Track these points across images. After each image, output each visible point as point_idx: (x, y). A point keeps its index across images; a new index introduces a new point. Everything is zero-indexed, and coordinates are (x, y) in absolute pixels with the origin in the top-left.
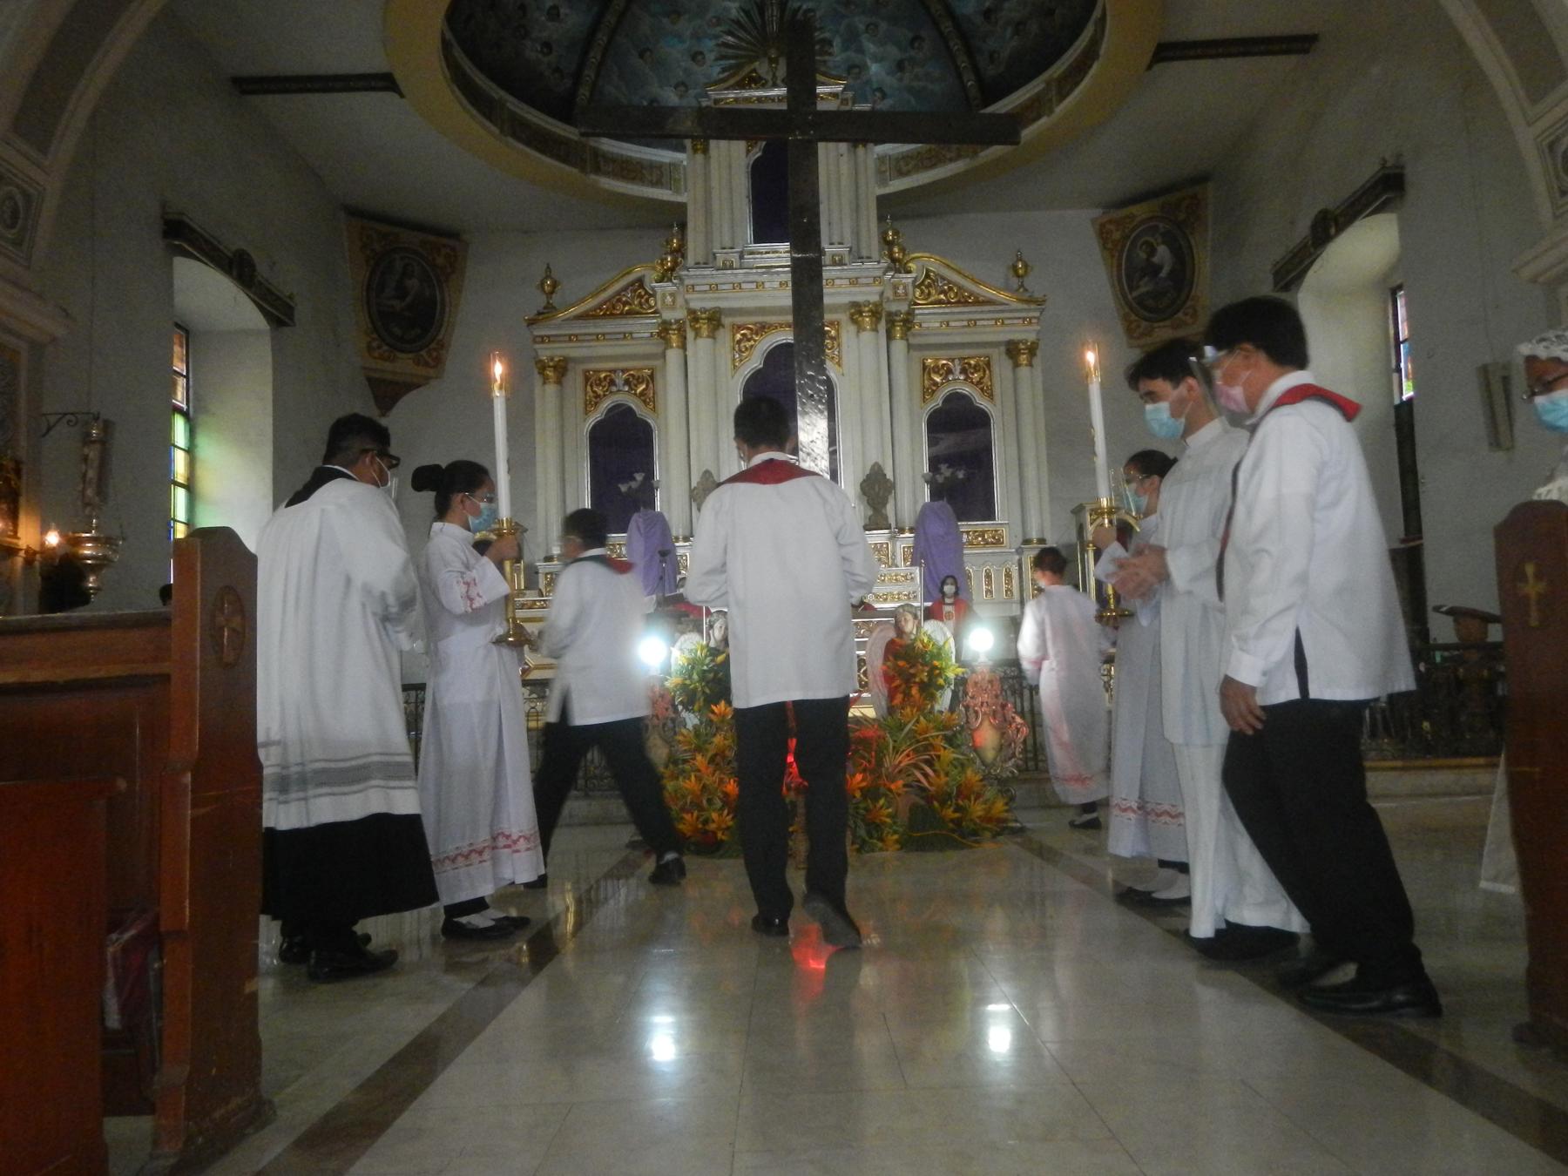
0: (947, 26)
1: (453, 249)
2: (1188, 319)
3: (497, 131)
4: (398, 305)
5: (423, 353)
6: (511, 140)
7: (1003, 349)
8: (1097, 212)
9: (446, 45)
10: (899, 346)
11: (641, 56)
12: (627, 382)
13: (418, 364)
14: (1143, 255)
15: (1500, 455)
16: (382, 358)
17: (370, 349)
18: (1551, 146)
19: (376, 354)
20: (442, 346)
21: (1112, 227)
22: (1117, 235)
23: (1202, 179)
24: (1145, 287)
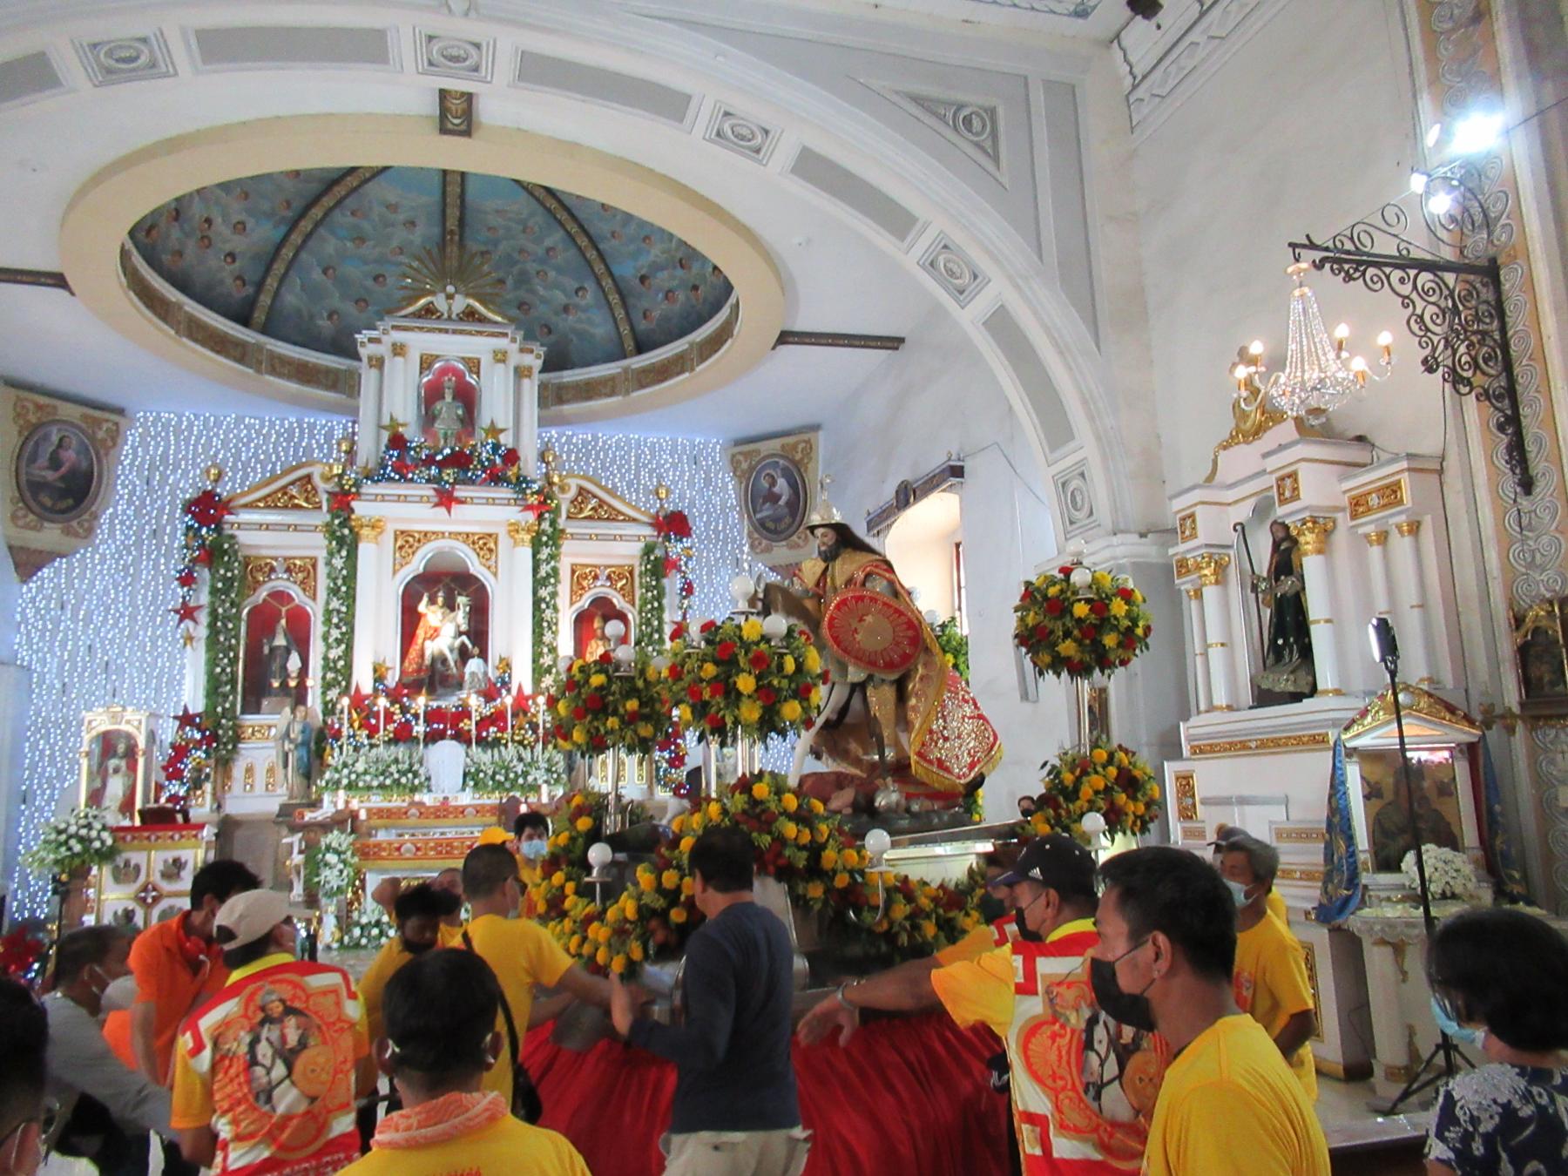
0: (607, 283)
1: (116, 424)
2: (801, 542)
3: (172, 332)
5: (74, 523)
6: (185, 340)
9: (124, 254)
11: (325, 272)
12: (288, 570)
15: (1027, 706)
16: (27, 527)
17: (14, 518)
18: (1064, 485)
19: (21, 523)
20: (96, 517)
21: (741, 458)
22: (745, 466)
23: (815, 428)
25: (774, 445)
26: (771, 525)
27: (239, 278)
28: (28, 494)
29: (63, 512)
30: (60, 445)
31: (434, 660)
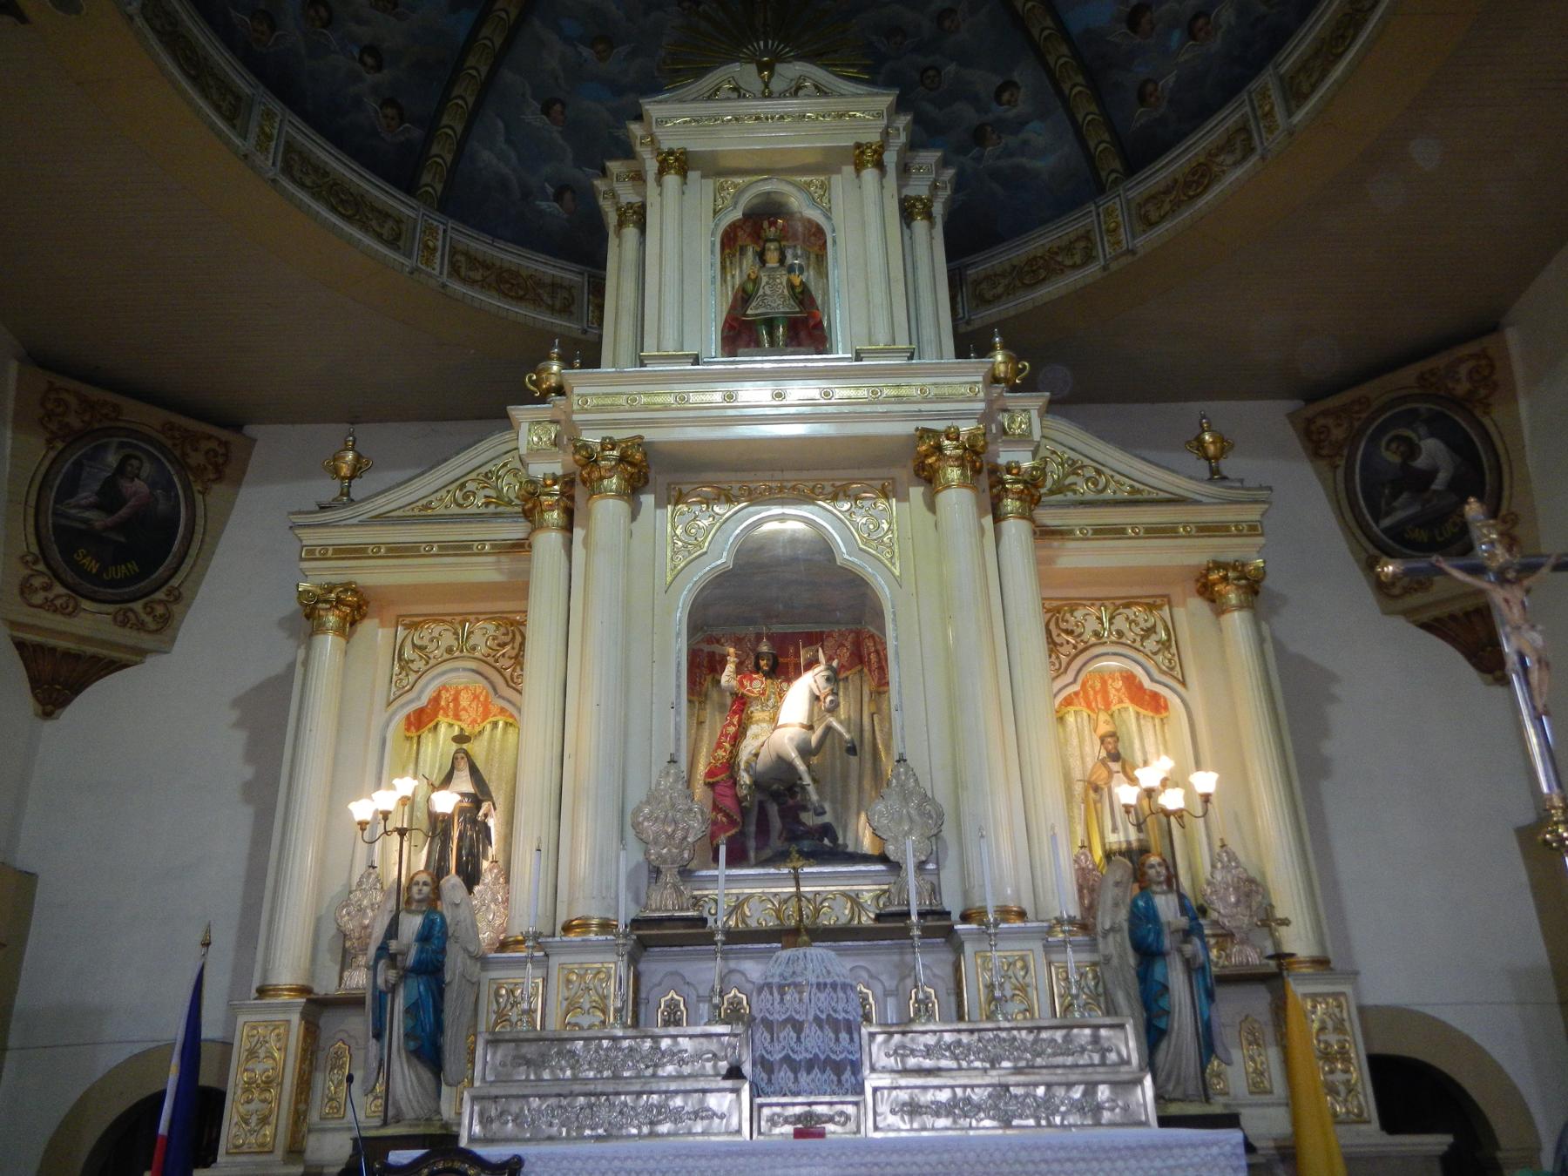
0: (1059, 55)
1: (226, 444)
4: (98, 519)
5: (138, 606)
7: (1192, 586)
8: (1299, 403)
10: (1015, 529)
11: (546, 110)
13: (123, 624)
14: (1395, 459)
17: (25, 588)
19: (38, 598)
20: (177, 597)
21: (1330, 422)
22: (1338, 434)
24: (1404, 510)
25: (1407, 376)
26: (1422, 536)
27: (388, 102)
28: (55, 553)
29: (113, 584)
30: (120, 470)
31: (758, 784)
